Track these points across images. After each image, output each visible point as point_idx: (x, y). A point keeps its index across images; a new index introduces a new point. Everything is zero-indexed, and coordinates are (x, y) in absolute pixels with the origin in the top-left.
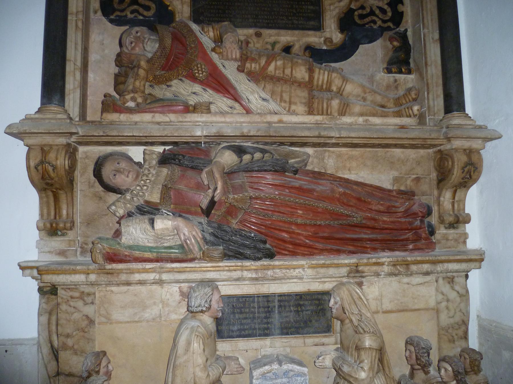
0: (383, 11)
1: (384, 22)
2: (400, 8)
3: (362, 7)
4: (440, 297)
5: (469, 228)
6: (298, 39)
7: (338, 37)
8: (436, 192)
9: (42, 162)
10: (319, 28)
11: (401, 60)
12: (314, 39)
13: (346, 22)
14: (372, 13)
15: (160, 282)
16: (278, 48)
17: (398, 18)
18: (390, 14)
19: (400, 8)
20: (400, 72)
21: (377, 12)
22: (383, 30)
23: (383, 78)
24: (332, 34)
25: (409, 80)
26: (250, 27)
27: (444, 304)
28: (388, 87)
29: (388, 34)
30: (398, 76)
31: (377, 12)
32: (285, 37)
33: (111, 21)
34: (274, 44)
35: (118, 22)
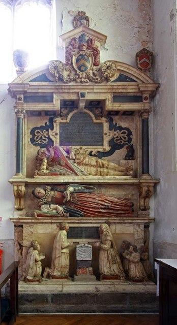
0: (125, 138)
1: (125, 142)
2: (131, 136)
3: (117, 137)
4: (135, 230)
5: (150, 211)
6: (95, 149)
7: (108, 148)
8: (139, 199)
9: (17, 190)
10: (102, 145)
11: (130, 155)
12: (100, 149)
13: (111, 142)
14: (121, 139)
15: (51, 223)
16: (88, 152)
17: (130, 140)
18: (127, 139)
19: (131, 136)
20: (129, 159)
21: (123, 139)
22: (124, 144)
23: (123, 162)
24: (107, 148)
25: (132, 163)
26: (78, 145)
27: (136, 232)
28: (125, 164)
29: (125, 146)
30: (129, 161)
31: (123, 139)
32: (90, 148)
33: (34, 145)
34: (86, 152)
35: (36, 145)
